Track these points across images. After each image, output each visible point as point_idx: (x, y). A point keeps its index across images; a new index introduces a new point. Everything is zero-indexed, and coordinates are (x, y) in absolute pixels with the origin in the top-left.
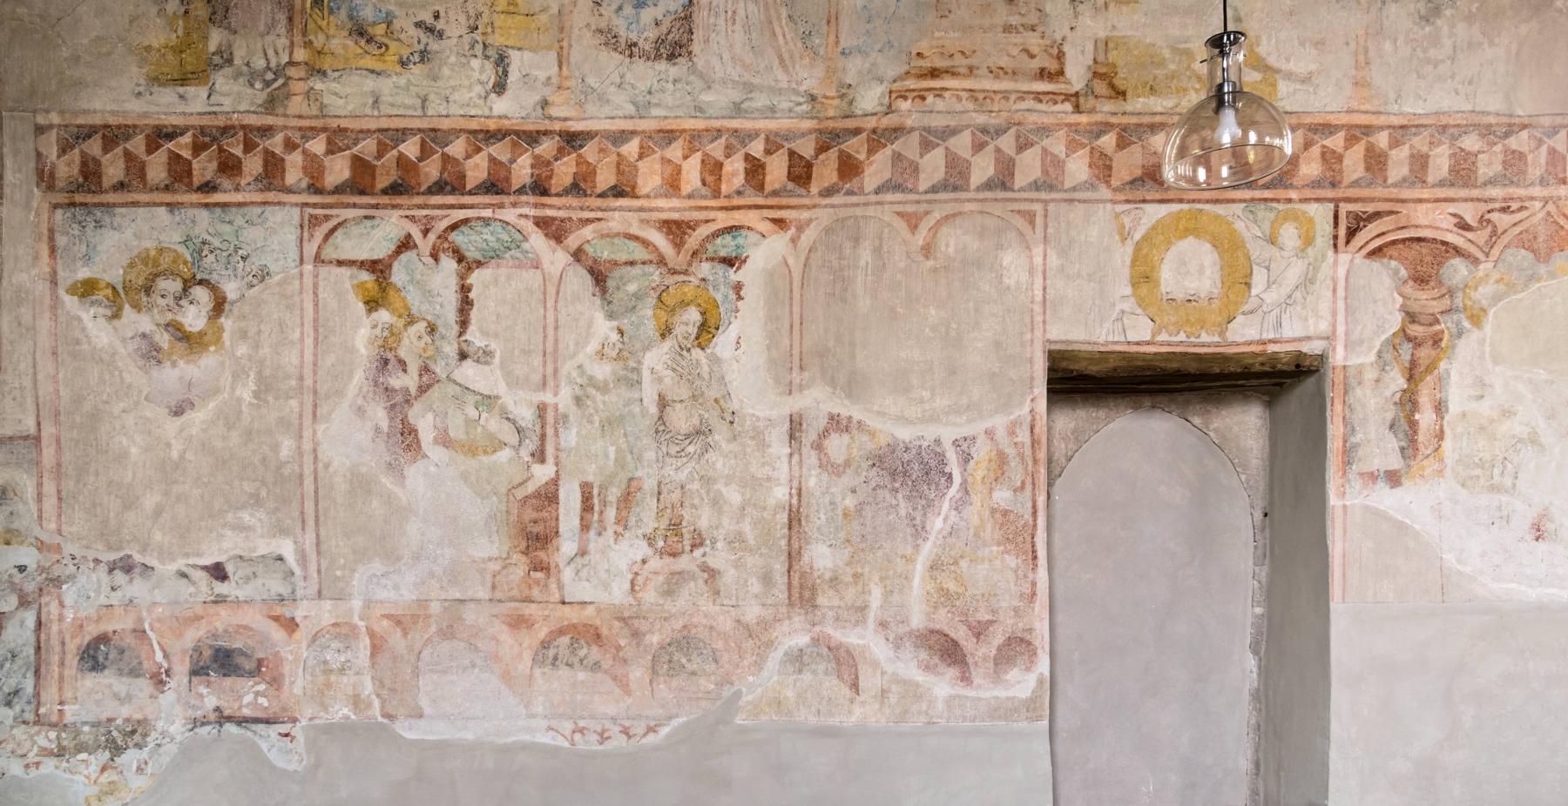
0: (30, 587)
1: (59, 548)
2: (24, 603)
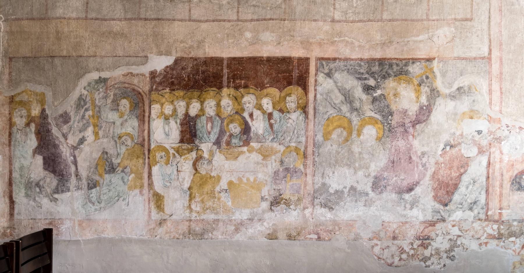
0: (484, 143)
1: (499, 121)
2: (481, 151)
